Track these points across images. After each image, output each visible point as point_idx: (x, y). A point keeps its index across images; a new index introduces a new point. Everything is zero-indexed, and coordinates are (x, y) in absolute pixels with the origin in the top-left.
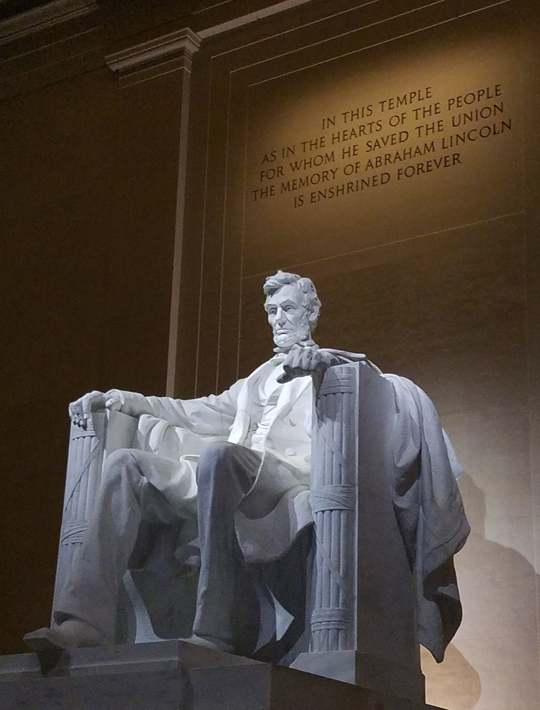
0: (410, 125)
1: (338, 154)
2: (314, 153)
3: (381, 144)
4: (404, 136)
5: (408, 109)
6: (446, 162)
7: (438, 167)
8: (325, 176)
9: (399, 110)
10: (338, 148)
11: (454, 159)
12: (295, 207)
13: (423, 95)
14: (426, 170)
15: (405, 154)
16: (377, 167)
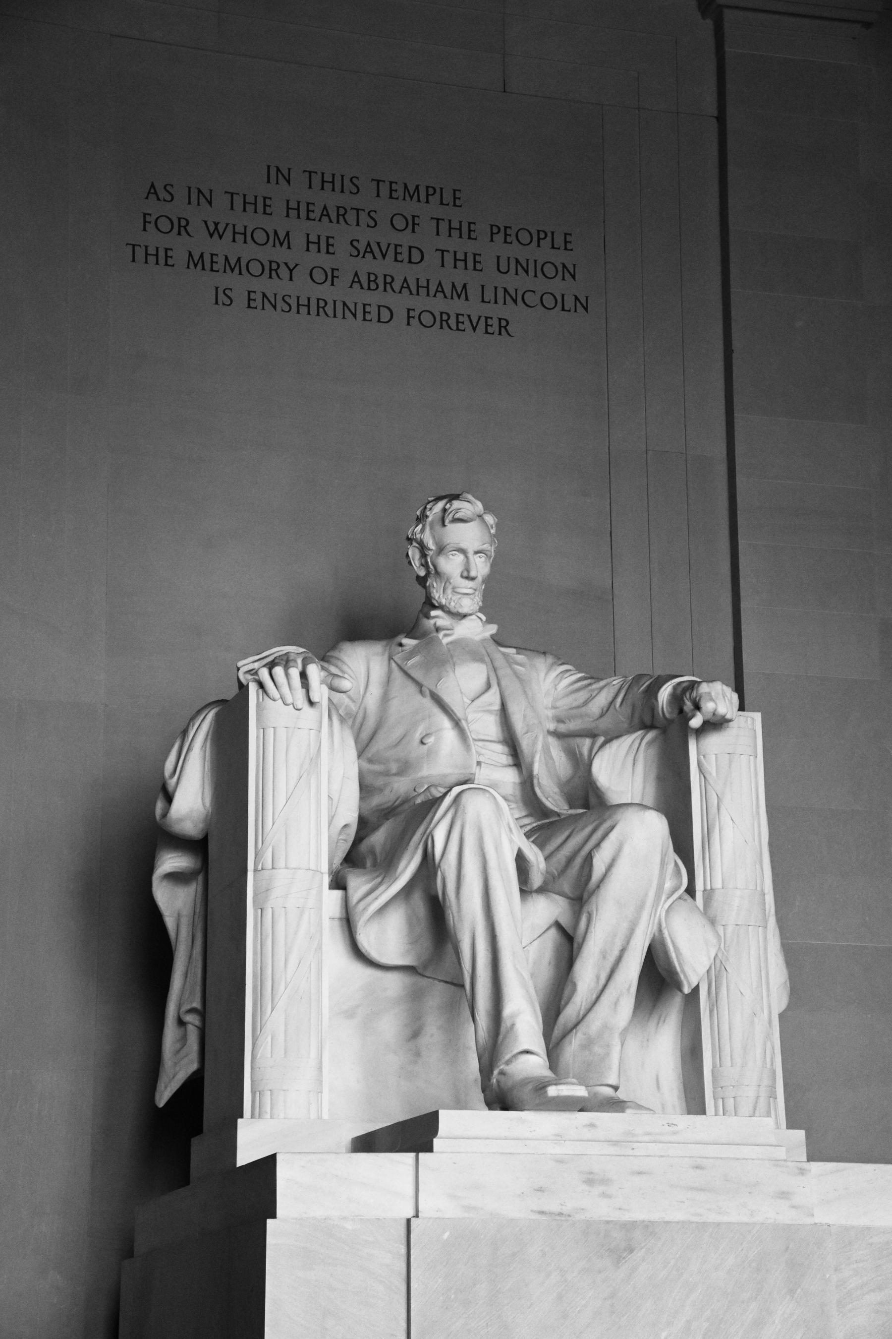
1: (299, 241)
4: (416, 256)
6: (487, 325)
7: (474, 329)
8: (272, 269)
10: (299, 229)
11: (500, 327)
12: (217, 303)
13: (448, 197)
14: (454, 327)
15: (418, 287)
16: (369, 288)
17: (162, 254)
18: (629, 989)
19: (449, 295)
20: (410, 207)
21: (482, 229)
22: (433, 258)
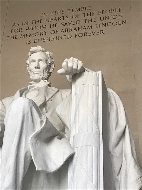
0: (81, 18)
1: (48, 26)
2: (37, 25)
3: (68, 24)
4: (78, 22)
5: (81, 13)
8: (41, 34)
9: (77, 13)
10: (48, 24)
17: (15, 37)
18: (9, 170)
19: (87, 28)
20: (77, 13)
21: (96, 13)
22: (83, 22)
